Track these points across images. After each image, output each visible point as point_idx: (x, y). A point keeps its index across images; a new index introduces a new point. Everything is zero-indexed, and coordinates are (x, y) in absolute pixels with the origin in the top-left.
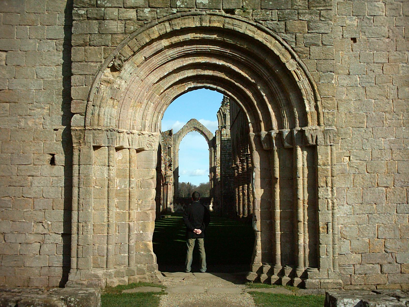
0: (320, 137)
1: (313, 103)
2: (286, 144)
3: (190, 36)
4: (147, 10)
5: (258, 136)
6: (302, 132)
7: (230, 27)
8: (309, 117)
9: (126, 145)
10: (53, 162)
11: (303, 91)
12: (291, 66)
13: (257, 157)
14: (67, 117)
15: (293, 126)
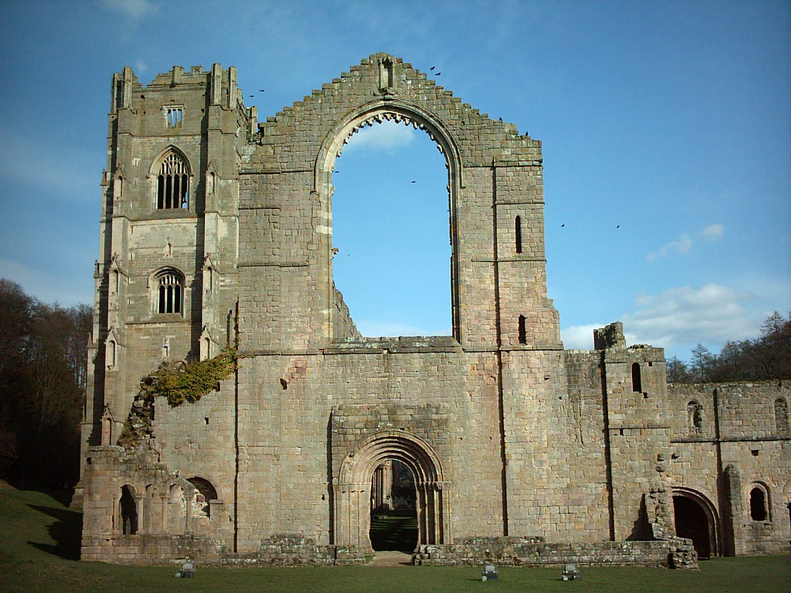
0: (443, 486)
1: (440, 471)
2: (430, 488)
3: (384, 440)
4: (365, 430)
5: (418, 484)
6: (435, 484)
7: (403, 437)
8: (438, 477)
9: (356, 490)
10: (323, 498)
11: (436, 466)
12: (430, 454)
13: (418, 493)
14: (330, 479)
15: (432, 481)
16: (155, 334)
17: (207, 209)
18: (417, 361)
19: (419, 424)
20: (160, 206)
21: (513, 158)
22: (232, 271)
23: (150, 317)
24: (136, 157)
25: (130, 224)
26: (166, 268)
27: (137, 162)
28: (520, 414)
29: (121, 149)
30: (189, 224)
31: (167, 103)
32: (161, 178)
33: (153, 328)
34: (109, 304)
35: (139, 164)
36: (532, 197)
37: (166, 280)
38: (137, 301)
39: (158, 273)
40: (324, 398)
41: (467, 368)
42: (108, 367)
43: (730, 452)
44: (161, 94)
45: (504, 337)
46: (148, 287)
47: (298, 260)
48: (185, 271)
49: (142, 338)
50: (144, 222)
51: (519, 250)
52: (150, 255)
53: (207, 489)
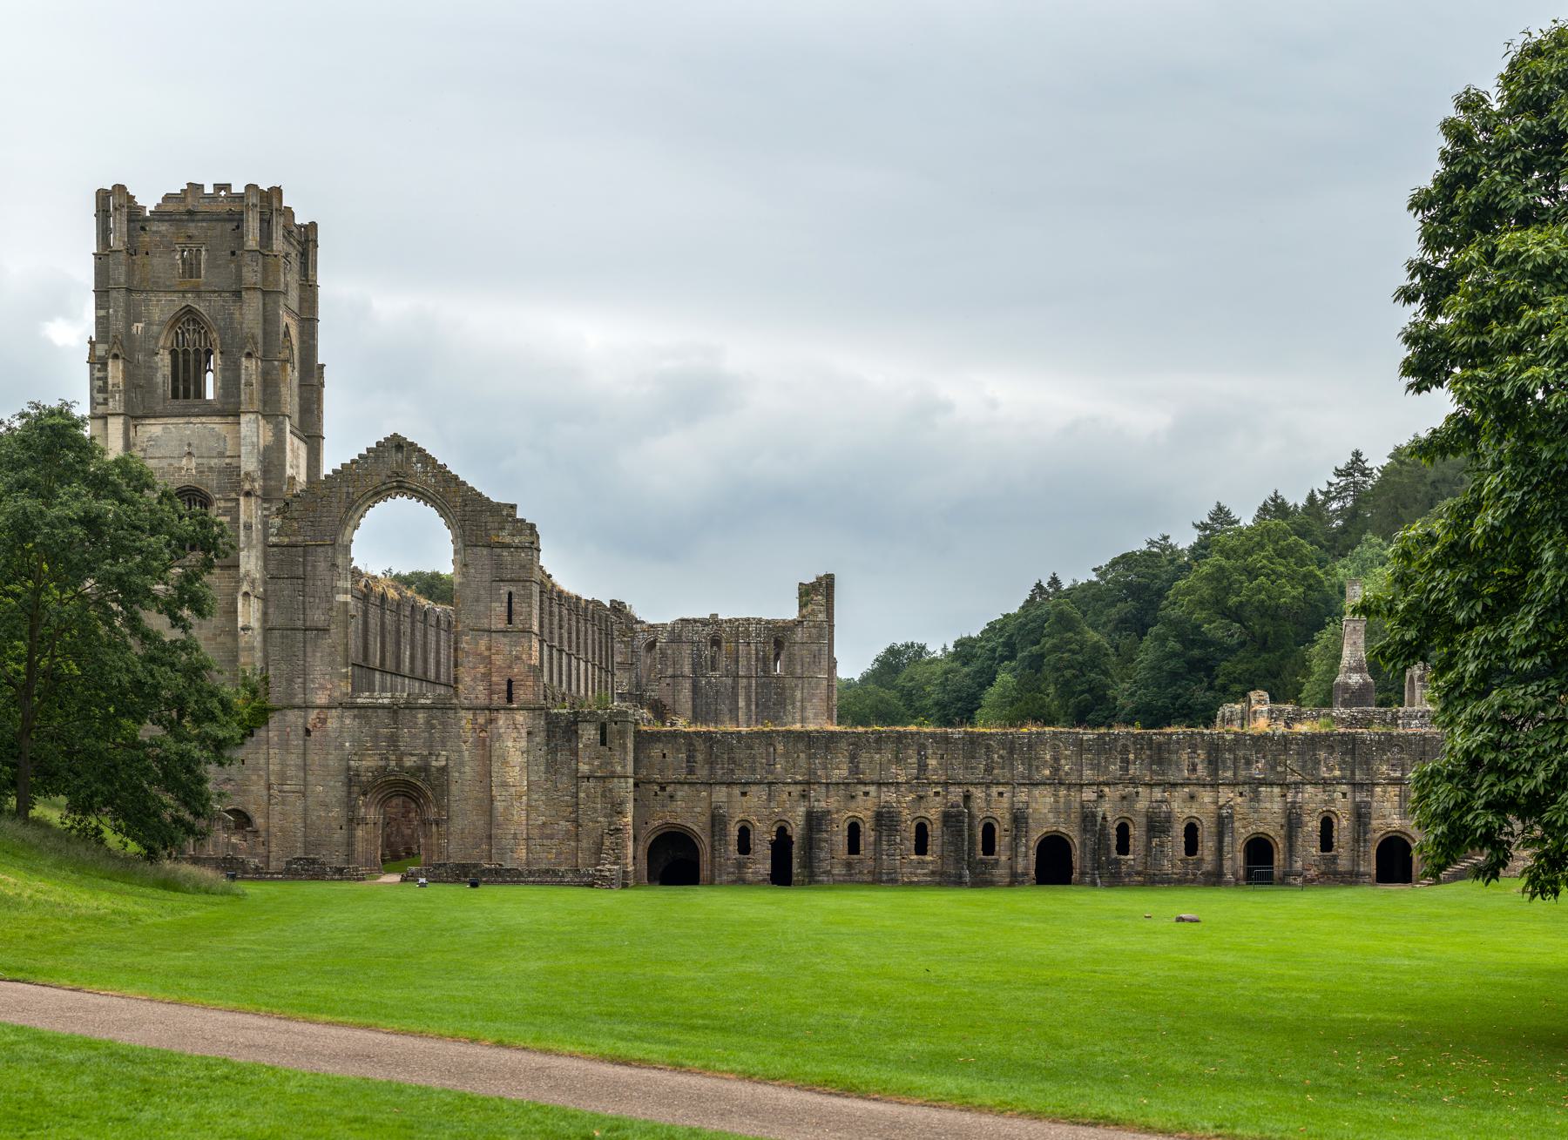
17: (243, 408)
18: (421, 717)
19: (419, 769)
20: (175, 396)
21: (508, 540)
25: (132, 423)
28: (505, 762)
32: (173, 353)
36: (523, 575)
40: (342, 745)
41: (463, 722)
43: (720, 794)
45: (495, 697)
47: (320, 625)
50: (152, 421)
51: (510, 622)
53: (242, 820)
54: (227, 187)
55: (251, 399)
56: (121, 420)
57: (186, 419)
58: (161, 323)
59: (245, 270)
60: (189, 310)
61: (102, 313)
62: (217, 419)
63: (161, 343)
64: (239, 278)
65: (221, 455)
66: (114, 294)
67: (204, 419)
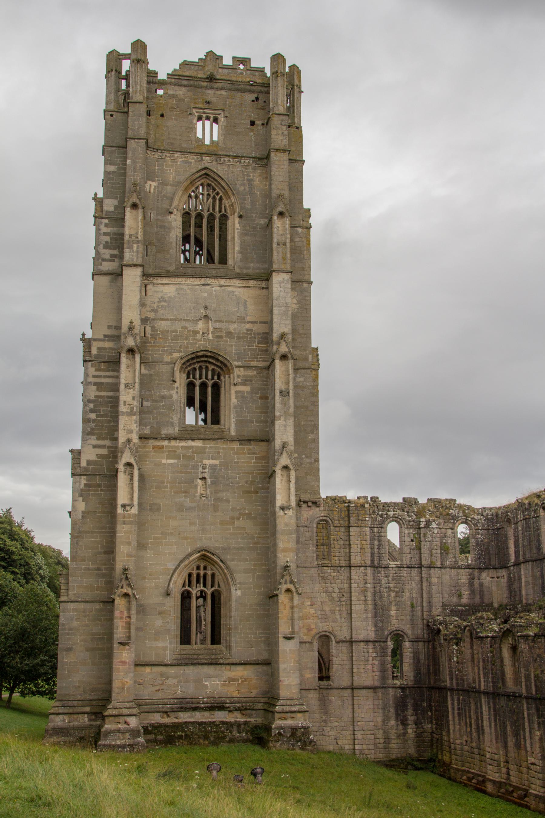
16: (185, 457)
17: (275, 267)
22: (307, 365)
23: (177, 429)
24: (149, 180)
26: (202, 353)
27: (153, 187)
29: (133, 162)
30: (237, 290)
31: (197, 106)
33: (182, 447)
34: (121, 403)
35: (154, 189)
37: (198, 372)
38: (156, 401)
39: (188, 361)
42: (124, 506)
44: (188, 91)
46: (174, 381)
48: (233, 361)
49: (164, 461)
50: (165, 281)
52: (176, 331)
54: (245, 61)
55: (284, 259)
56: (138, 272)
57: (204, 281)
58: (176, 184)
59: (274, 132)
60: (206, 174)
61: (112, 168)
62: (238, 282)
63: (175, 203)
64: (267, 138)
65: (241, 320)
66: (131, 144)
67: (222, 282)
